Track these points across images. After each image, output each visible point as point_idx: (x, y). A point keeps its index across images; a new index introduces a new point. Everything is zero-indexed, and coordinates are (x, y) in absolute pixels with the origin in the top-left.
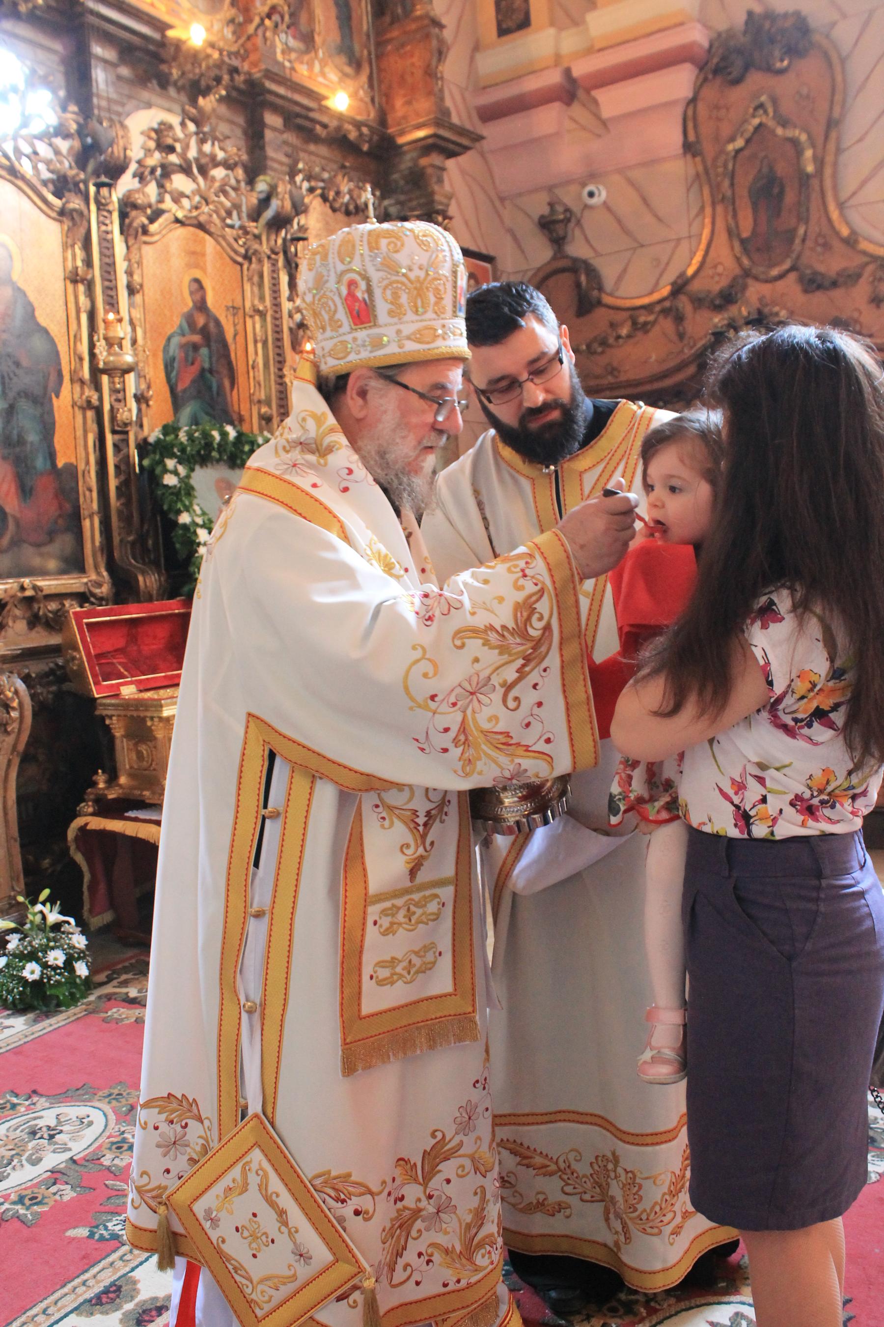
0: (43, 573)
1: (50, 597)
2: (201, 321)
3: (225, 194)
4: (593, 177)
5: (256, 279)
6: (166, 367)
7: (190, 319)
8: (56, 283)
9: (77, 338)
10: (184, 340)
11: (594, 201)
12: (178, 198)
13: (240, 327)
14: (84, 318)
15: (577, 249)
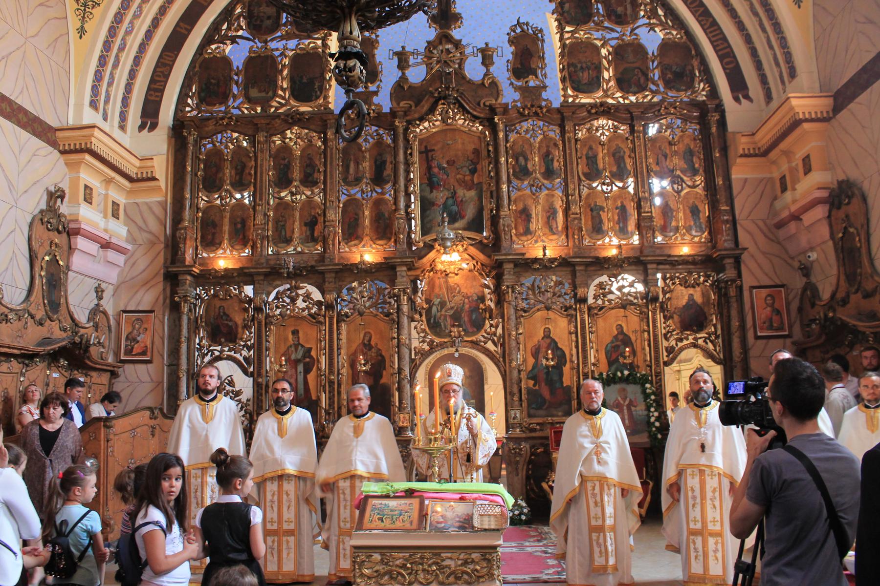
0: (558, 416)
1: (557, 423)
2: (620, 337)
3: (631, 295)
4: (812, 249)
5: (645, 320)
6: (606, 353)
7: (616, 337)
8: (565, 335)
9: (571, 350)
10: (613, 345)
11: (811, 259)
12: (610, 301)
13: (639, 337)
14: (573, 343)
15: (813, 279)
